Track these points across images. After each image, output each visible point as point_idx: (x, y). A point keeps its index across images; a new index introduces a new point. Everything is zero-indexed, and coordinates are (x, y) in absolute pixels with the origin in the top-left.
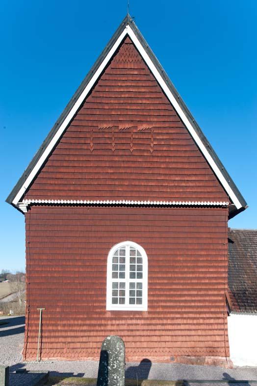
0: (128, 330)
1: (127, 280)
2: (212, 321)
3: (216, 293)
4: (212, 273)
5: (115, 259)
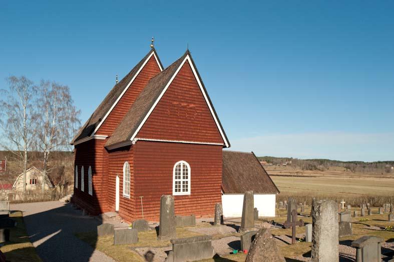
0: (183, 205)
1: (182, 180)
2: (216, 198)
3: (217, 185)
4: (216, 176)
5: (176, 170)
